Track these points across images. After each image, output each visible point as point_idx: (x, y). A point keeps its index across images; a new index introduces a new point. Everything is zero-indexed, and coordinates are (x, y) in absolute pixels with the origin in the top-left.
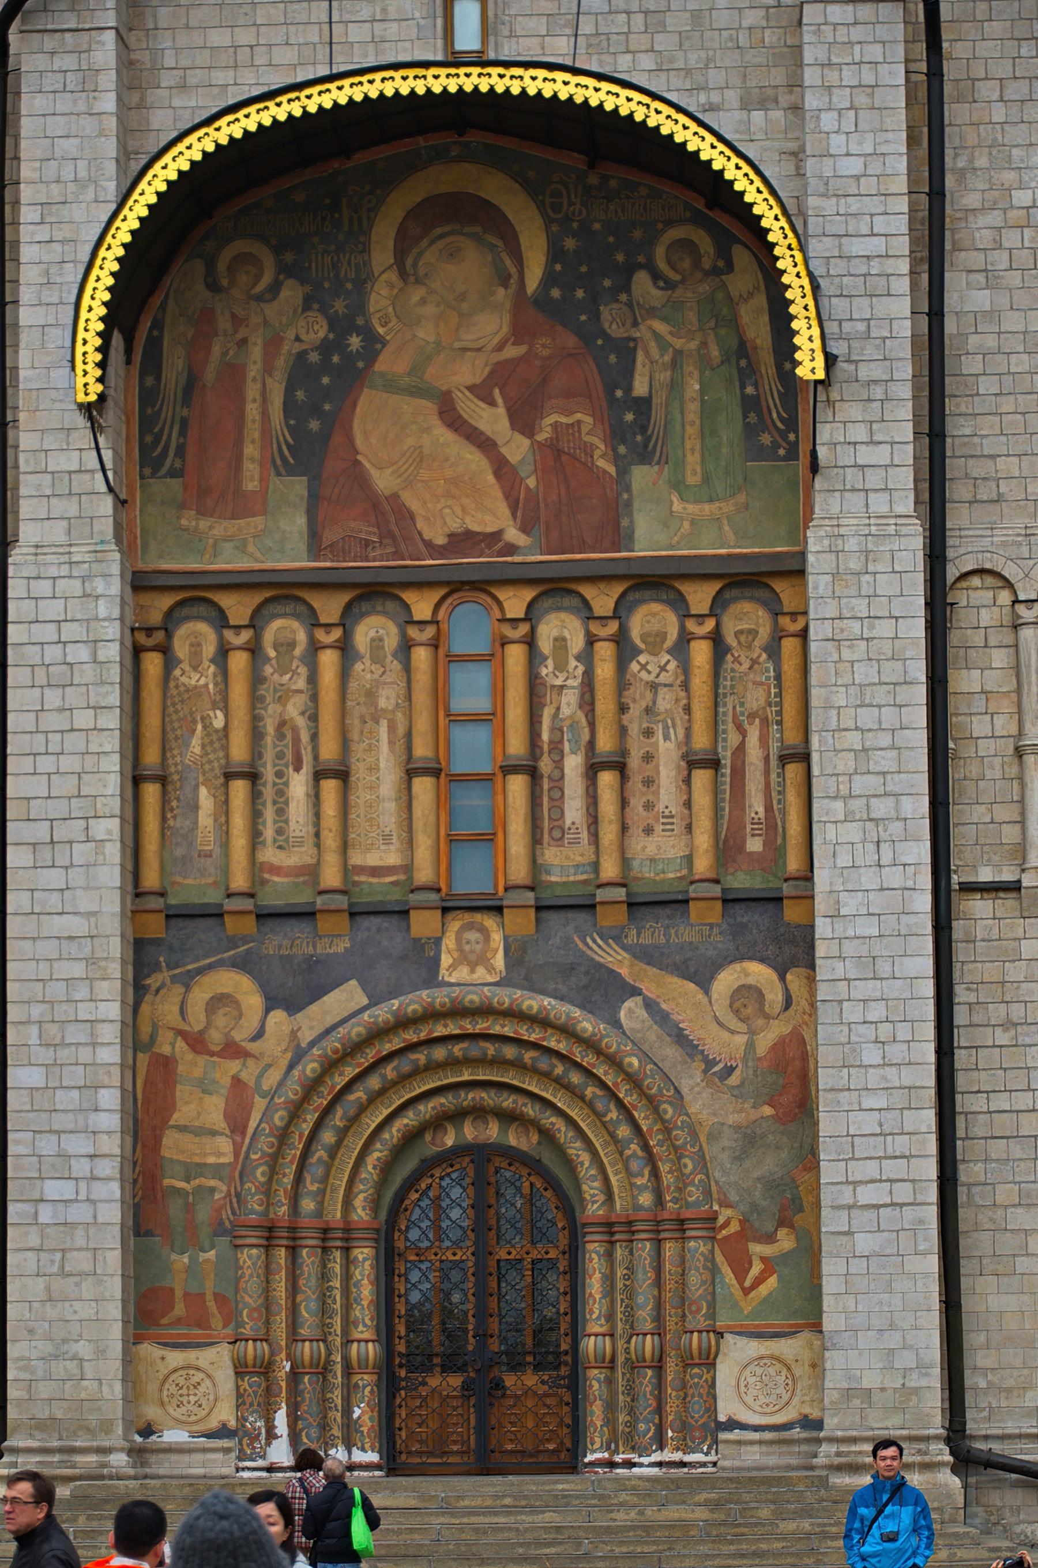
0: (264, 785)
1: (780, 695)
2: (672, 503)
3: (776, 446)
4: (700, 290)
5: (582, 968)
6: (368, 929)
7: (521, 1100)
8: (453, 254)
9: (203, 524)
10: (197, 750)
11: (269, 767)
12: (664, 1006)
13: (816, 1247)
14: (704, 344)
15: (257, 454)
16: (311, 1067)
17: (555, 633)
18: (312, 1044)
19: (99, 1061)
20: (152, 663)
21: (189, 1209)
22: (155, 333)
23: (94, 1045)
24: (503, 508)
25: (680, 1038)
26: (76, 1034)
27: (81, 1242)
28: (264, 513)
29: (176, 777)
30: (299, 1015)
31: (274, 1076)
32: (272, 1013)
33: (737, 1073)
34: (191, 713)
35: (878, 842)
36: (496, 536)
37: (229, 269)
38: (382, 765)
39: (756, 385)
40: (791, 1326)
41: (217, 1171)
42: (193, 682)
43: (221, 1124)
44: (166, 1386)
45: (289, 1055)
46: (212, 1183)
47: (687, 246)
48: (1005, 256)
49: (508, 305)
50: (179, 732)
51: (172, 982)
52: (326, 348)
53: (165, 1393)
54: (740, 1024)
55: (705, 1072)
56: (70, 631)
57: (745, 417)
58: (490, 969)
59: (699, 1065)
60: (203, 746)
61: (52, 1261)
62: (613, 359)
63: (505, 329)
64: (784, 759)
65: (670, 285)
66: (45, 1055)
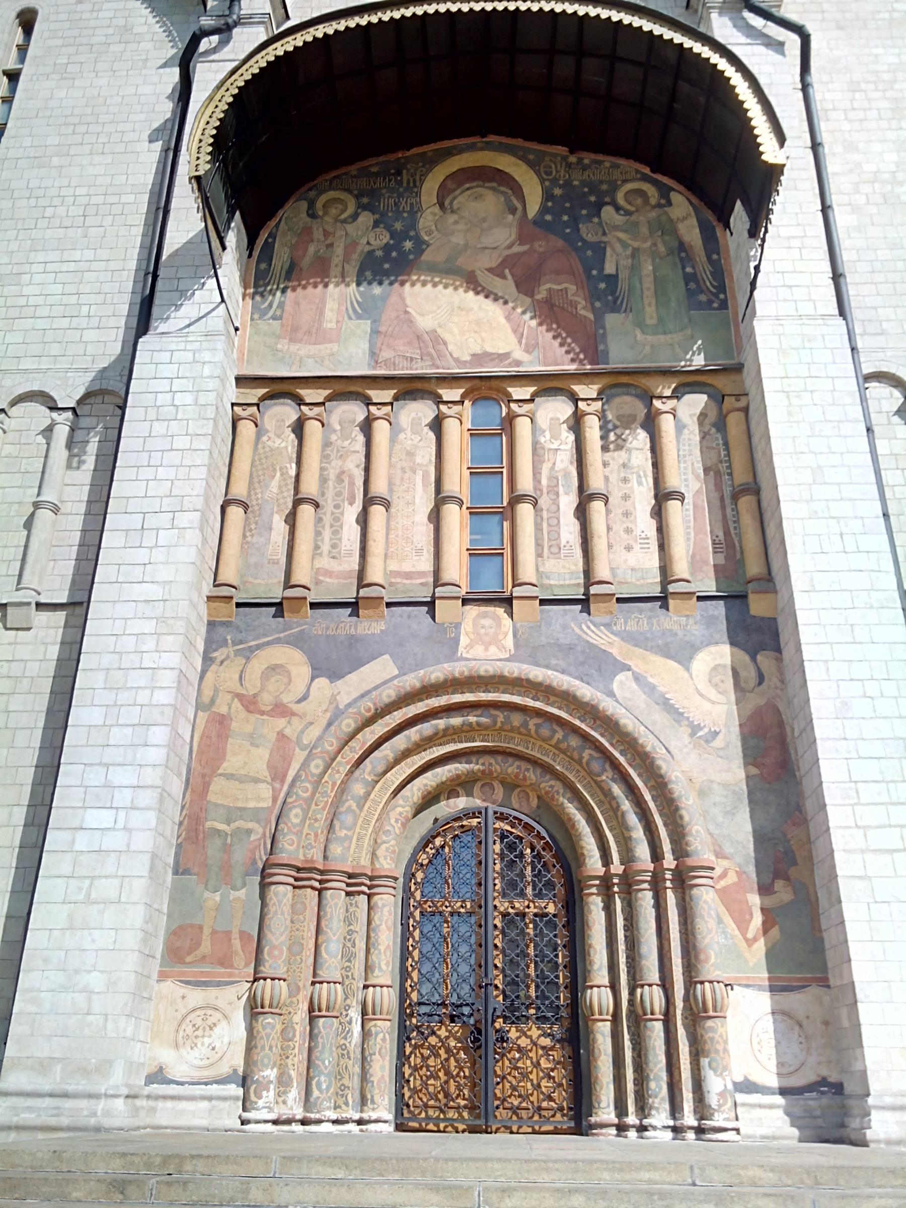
0: (325, 514)
1: (728, 455)
2: (636, 337)
3: (710, 302)
4: (650, 215)
5: (579, 648)
6: (401, 616)
7: (524, 765)
8: (478, 198)
9: (294, 348)
10: (275, 490)
11: (329, 501)
12: (651, 680)
13: (813, 899)
14: (655, 244)
15: (336, 306)
16: (348, 724)
17: (551, 415)
18: (349, 705)
19: (154, 702)
20: (246, 429)
21: (227, 849)
22: (270, 240)
23: (153, 689)
24: (513, 339)
25: (666, 705)
26: (138, 679)
27: (110, 869)
28: (338, 341)
29: (256, 508)
30: (339, 683)
31: (314, 733)
32: (317, 680)
33: (720, 737)
34: (273, 465)
35: (841, 535)
36: (507, 355)
37: (324, 206)
38: (417, 501)
39: (693, 268)
40: (799, 979)
41: (255, 816)
42: (276, 445)
43: (265, 774)
44: (183, 1027)
45: (328, 715)
46: (250, 825)
47: (641, 193)
48: (864, 197)
49: (515, 223)
50: (262, 478)
51: (235, 655)
52: (387, 248)
53: (181, 1033)
54: (720, 696)
55: (692, 735)
56: (177, 385)
57: (687, 284)
58: (502, 648)
59: (685, 731)
60: (280, 487)
61: (80, 889)
62: (589, 253)
63: (513, 237)
64: (735, 497)
65: (628, 213)
66: (106, 697)
